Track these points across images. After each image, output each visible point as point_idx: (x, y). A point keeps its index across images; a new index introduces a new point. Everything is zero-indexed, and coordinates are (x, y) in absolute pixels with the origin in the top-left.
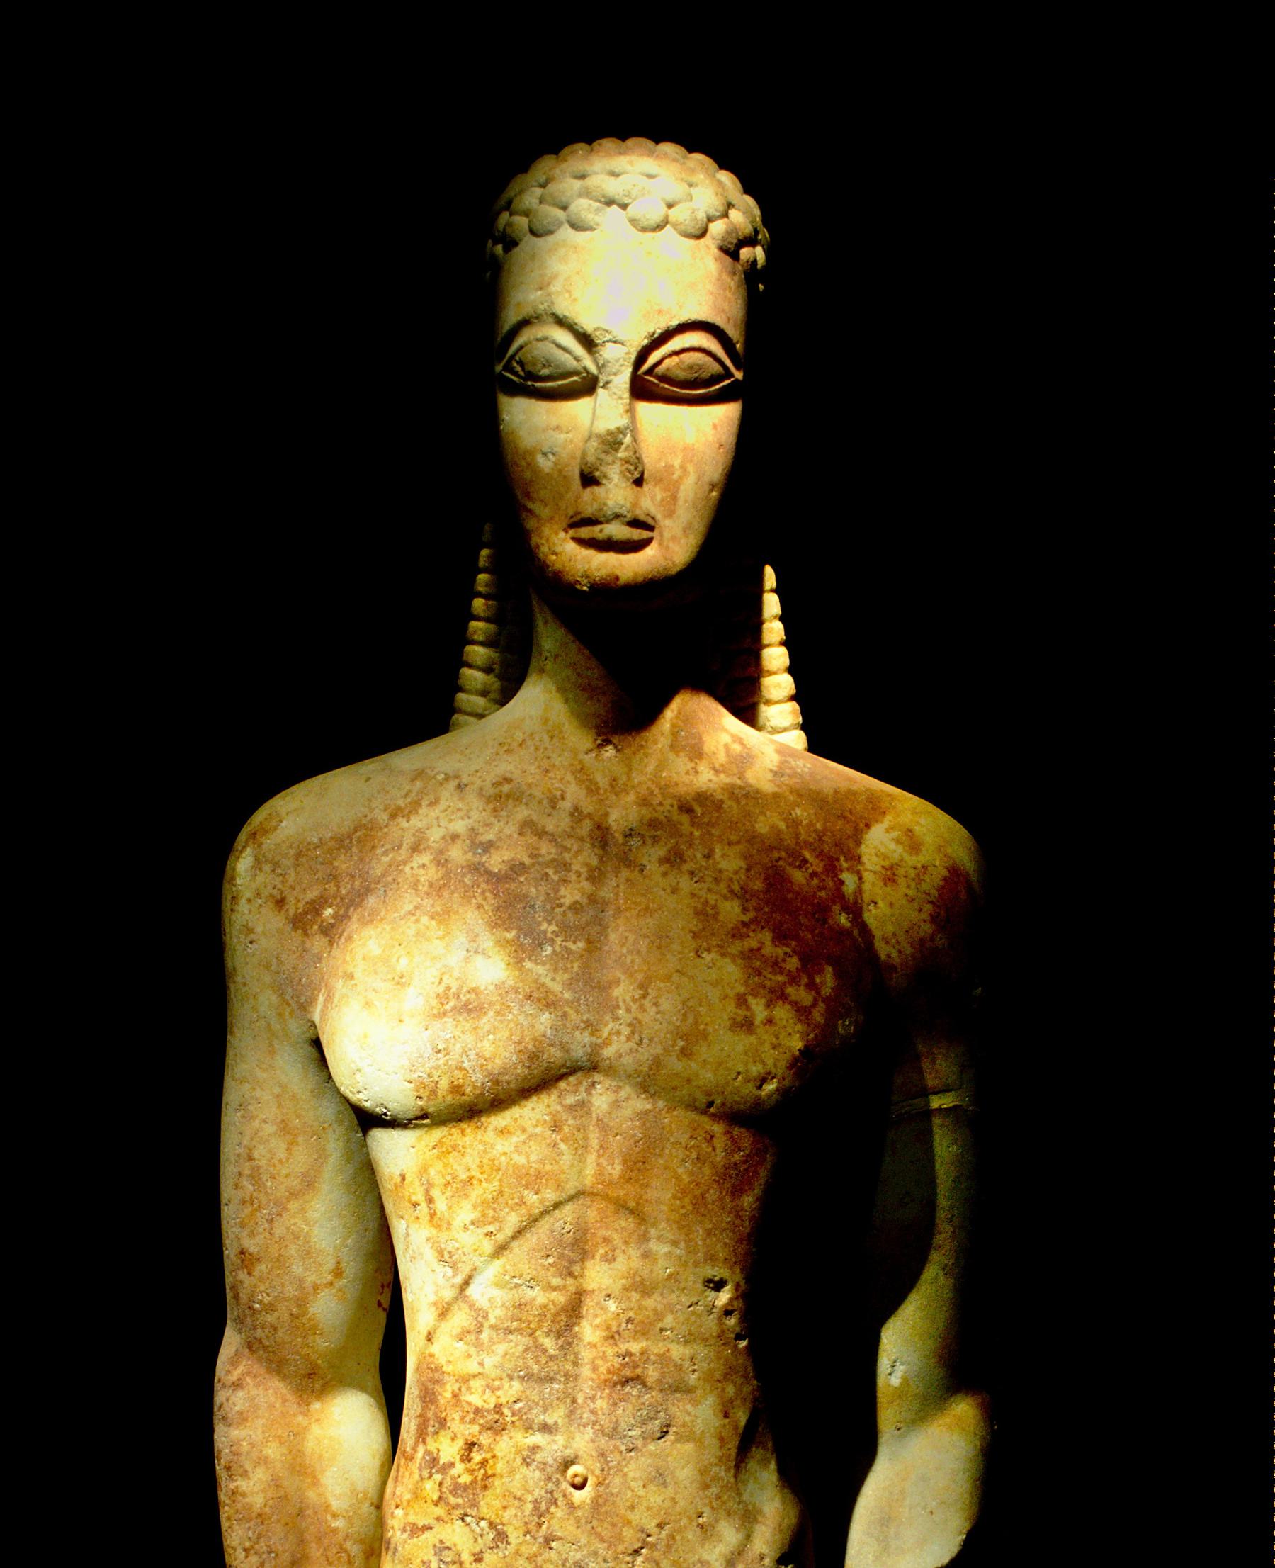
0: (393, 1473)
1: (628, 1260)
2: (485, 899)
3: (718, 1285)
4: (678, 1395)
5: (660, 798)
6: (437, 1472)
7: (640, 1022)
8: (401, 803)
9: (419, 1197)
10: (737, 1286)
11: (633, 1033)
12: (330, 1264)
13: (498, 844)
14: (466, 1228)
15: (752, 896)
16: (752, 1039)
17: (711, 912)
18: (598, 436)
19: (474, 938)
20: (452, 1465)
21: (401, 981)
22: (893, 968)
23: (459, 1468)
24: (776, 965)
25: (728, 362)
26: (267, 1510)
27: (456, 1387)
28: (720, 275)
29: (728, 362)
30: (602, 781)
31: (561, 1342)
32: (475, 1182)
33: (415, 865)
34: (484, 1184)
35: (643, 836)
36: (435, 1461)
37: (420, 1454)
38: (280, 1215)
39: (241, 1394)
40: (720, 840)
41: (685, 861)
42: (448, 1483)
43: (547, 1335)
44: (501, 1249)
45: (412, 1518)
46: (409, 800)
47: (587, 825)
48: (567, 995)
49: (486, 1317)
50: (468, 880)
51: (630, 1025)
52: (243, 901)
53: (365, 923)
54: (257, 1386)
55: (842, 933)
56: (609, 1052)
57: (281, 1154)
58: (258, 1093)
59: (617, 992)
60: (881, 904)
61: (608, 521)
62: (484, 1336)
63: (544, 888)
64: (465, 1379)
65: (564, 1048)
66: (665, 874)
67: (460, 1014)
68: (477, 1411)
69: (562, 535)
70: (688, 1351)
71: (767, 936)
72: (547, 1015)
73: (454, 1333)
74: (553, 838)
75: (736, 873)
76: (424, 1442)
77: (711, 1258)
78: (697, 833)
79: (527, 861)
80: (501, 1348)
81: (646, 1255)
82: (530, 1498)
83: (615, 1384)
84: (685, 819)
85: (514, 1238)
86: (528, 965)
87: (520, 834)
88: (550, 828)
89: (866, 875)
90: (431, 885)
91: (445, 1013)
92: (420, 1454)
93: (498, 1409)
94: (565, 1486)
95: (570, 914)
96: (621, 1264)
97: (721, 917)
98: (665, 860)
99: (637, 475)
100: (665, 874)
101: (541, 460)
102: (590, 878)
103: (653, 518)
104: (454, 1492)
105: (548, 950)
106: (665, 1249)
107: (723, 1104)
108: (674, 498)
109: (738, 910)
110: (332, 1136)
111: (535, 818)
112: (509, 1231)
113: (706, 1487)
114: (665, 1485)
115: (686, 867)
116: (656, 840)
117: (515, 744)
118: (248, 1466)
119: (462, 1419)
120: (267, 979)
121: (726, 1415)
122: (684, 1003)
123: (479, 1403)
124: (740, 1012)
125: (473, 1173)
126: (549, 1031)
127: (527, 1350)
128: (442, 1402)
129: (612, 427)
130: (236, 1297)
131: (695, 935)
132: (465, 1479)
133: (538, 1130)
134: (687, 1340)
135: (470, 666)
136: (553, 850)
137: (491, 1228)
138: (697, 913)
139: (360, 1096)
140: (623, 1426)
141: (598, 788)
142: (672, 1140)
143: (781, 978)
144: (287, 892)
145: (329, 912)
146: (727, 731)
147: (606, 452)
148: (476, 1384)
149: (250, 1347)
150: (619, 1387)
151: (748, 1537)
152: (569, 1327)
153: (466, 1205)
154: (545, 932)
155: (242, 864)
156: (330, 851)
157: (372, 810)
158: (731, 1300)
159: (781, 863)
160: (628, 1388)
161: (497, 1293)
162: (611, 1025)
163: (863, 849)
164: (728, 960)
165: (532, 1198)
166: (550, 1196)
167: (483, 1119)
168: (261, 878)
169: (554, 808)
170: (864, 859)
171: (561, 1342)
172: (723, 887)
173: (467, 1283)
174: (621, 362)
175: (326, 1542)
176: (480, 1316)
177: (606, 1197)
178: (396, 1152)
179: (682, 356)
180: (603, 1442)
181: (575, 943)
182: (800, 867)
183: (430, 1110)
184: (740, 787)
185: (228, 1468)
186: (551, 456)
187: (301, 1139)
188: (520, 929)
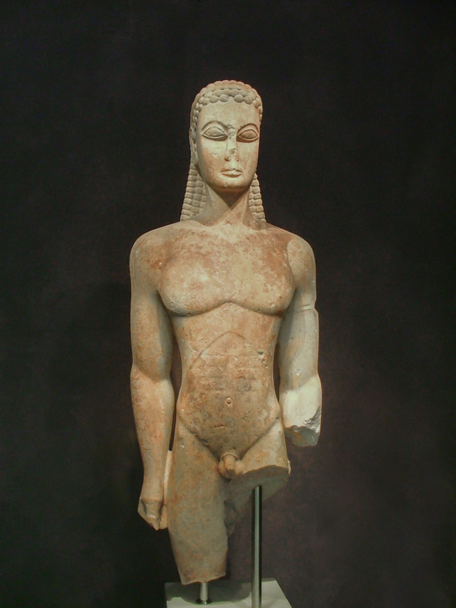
1: (240, 348)
3: (261, 353)
8: (178, 237)
12: (161, 349)
14: (200, 341)
21: (182, 281)
24: (272, 276)
39: (139, 381)
42: (196, 403)
44: (209, 346)
49: (205, 363)
50: (197, 255)
55: (285, 268)
56: (234, 298)
59: (235, 283)
62: (205, 367)
64: (200, 378)
65: (223, 297)
68: (204, 385)
71: (269, 269)
77: (259, 347)
78: (251, 244)
79: (211, 251)
81: (244, 347)
84: (248, 241)
85: (212, 343)
86: (213, 276)
91: (194, 289)
92: (188, 396)
93: (209, 385)
94: (226, 403)
96: (238, 349)
98: (243, 251)
102: (226, 255)
105: (217, 273)
106: (249, 345)
112: (211, 341)
114: (250, 402)
115: (250, 252)
116: (241, 246)
127: (216, 370)
131: (253, 269)
132: (201, 402)
134: (255, 367)
135: (186, 203)
140: (239, 388)
151: (269, 414)
155: (136, 251)
156: (160, 249)
163: (288, 248)
165: (216, 333)
166: (221, 333)
167: (204, 314)
173: (200, 354)
178: (186, 323)
183: (191, 312)
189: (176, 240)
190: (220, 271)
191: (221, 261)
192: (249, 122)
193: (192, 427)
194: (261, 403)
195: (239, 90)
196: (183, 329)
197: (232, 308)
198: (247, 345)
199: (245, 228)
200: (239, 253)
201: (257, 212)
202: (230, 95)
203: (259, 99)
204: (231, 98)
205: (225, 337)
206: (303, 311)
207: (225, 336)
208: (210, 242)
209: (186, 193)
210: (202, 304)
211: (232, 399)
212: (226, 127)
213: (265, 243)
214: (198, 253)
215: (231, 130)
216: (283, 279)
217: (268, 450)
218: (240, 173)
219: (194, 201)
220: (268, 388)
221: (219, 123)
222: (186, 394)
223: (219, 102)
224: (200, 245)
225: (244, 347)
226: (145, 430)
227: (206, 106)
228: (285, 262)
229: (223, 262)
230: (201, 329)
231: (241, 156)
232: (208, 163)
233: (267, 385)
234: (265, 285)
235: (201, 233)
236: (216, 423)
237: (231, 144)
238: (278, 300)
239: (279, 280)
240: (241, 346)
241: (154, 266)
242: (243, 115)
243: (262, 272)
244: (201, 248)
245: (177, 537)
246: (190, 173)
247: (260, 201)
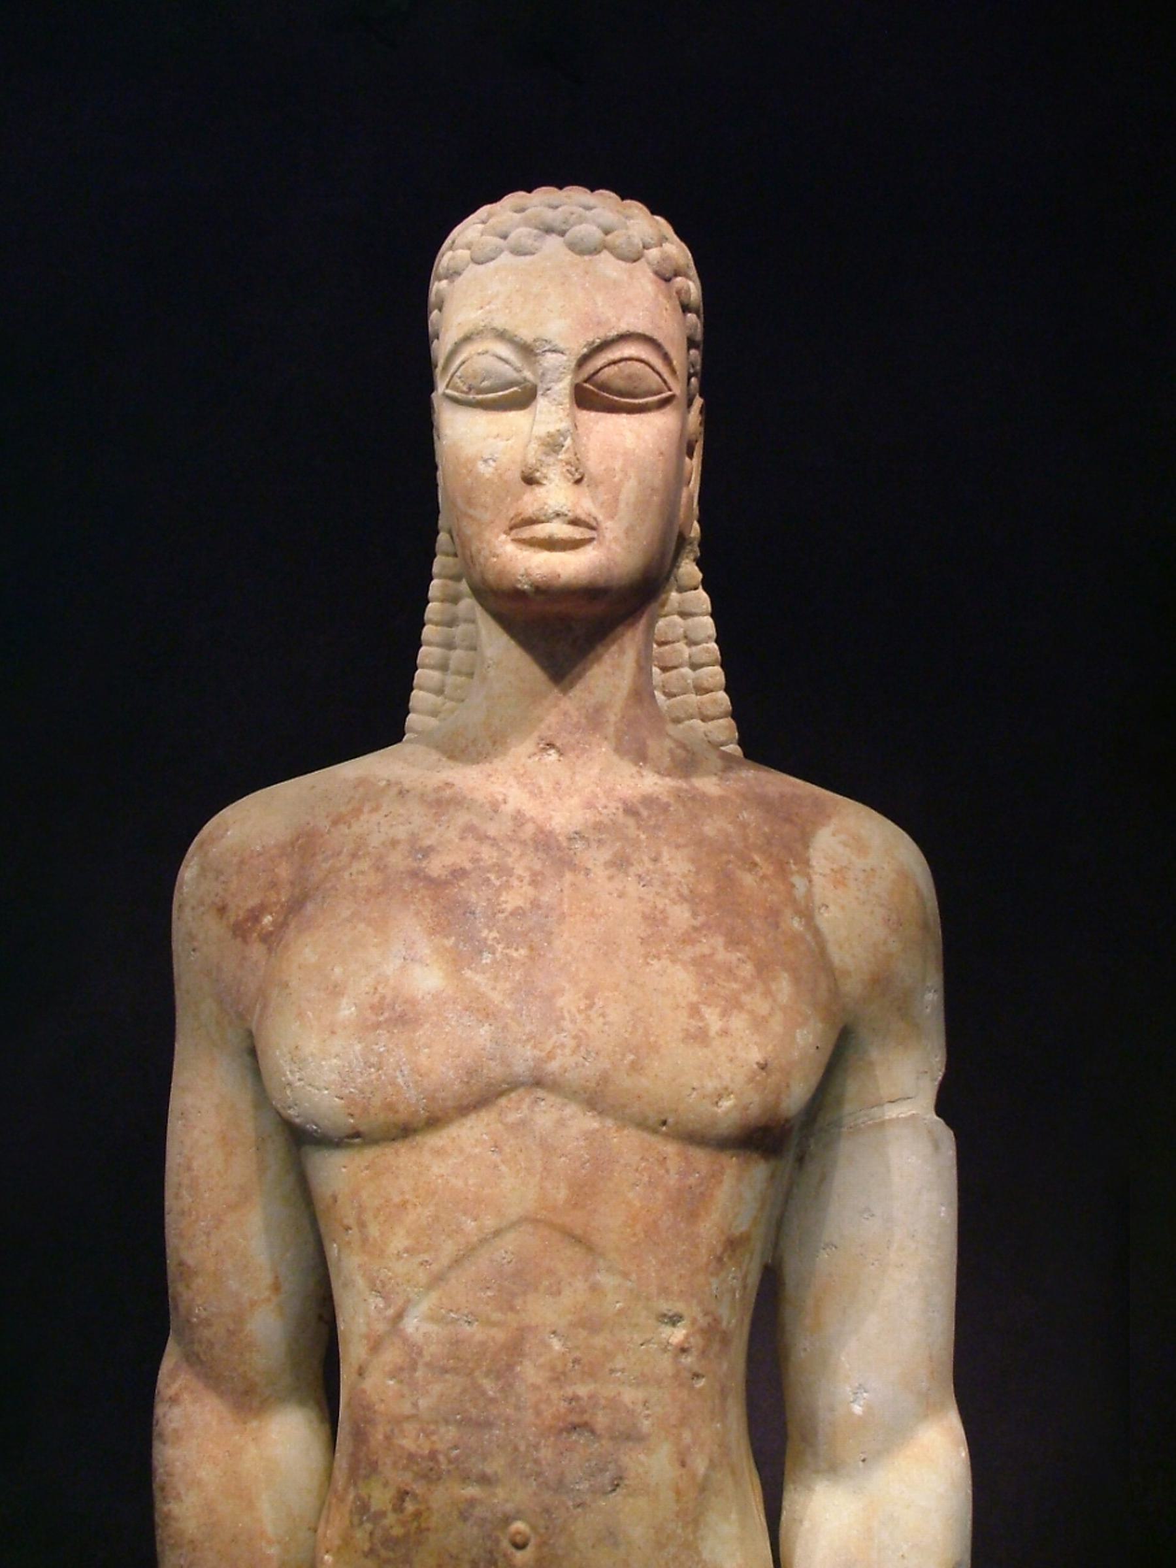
0: (325, 1512)
1: (575, 1293)
2: (424, 904)
3: (674, 1320)
4: (631, 1444)
5: (604, 801)
6: (368, 1520)
7: (586, 1034)
8: (343, 809)
10: (694, 1321)
11: (578, 1046)
12: (267, 1279)
13: (440, 849)
15: (702, 900)
17: (659, 916)
18: (539, 438)
20: (382, 1514)
21: (336, 991)
22: (847, 973)
23: (391, 1519)
24: (730, 972)
25: (666, 375)
27: (388, 1428)
28: (656, 296)
29: (666, 375)
30: (545, 784)
31: (500, 1384)
32: (409, 1206)
33: (354, 870)
34: (419, 1209)
35: (587, 840)
38: (217, 1228)
41: (632, 865)
42: (379, 1533)
43: (487, 1374)
44: (437, 1280)
46: (350, 807)
48: (509, 1006)
49: (420, 1354)
51: (575, 1037)
52: (187, 910)
55: (794, 940)
56: (553, 1066)
59: (561, 1002)
60: (832, 908)
61: (548, 521)
64: (398, 1421)
65: (505, 1062)
66: (611, 878)
67: (395, 1026)
68: (411, 1457)
69: (503, 537)
70: (640, 1395)
71: (719, 941)
72: (486, 1027)
73: (387, 1369)
74: (494, 842)
75: (684, 876)
76: (355, 1484)
77: (664, 1291)
78: (643, 837)
79: (468, 866)
80: (437, 1388)
81: (594, 1288)
83: (561, 1431)
84: (631, 822)
86: (468, 973)
87: (462, 839)
88: (492, 832)
89: (815, 878)
90: (369, 891)
91: (378, 1026)
92: (351, 1497)
93: (433, 1456)
94: (505, 1544)
96: (568, 1298)
97: (670, 922)
99: (577, 476)
100: (611, 878)
101: (481, 467)
102: (534, 883)
103: (595, 519)
105: (487, 958)
107: (677, 1123)
108: (616, 500)
109: (687, 915)
112: (445, 1261)
113: (661, 1546)
114: (616, 1544)
115: (633, 870)
116: (600, 842)
118: (181, 1488)
119: (395, 1463)
122: (632, 1013)
124: (693, 1022)
125: (407, 1197)
126: (488, 1045)
127: (464, 1391)
129: (552, 429)
130: (176, 1307)
131: (643, 941)
132: (397, 1531)
134: (642, 1381)
135: (421, 688)
136: (495, 854)
137: (426, 1257)
138: (645, 917)
139: (291, 1112)
141: (541, 792)
142: (622, 1161)
145: (267, 919)
146: (670, 736)
147: (547, 454)
148: (410, 1428)
149: (187, 1360)
150: (565, 1434)
152: (510, 1367)
154: (486, 939)
155: (189, 872)
158: (687, 1337)
159: (730, 866)
160: (574, 1437)
161: (432, 1328)
162: (555, 1037)
164: (678, 967)
165: (470, 1225)
167: (418, 1138)
169: (496, 811)
170: (814, 863)
171: (500, 1384)
173: (400, 1316)
174: (561, 369)
176: (414, 1352)
177: (551, 1225)
179: (622, 364)
180: (547, 1496)
181: (517, 950)
182: (750, 870)
183: (363, 1128)
184: (686, 791)
185: (162, 1489)
186: (491, 462)
190: (500, 947)
191: (509, 907)
192: (623, 327)
194: (672, 1550)
195: (588, 208)
196: (335, 1199)
197: (546, 1114)
198: (607, 1280)
199: (626, 768)
200: (588, 871)
201: (705, 719)
202: (549, 230)
203: (677, 250)
204: (554, 241)
205: (510, 1242)
206: (882, 1124)
207: (510, 1236)
208: (470, 829)
209: (423, 649)
210: (412, 1094)
211: (534, 1528)
212: (528, 351)
214: (414, 874)
215: (550, 360)
216: (784, 987)
218: (593, 534)
219: (451, 679)
220: (706, 1477)
221: (502, 335)
222: (346, 1490)
223: (506, 258)
224: (427, 843)
225: (594, 1288)
227: (459, 280)
229: (517, 913)
230: (404, 1204)
231: (594, 464)
232: (460, 502)
233: (700, 1465)
235: (438, 789)
237: (551, 413)
238: (751, 1080)
239: (760, 988)
240: (580, 1284)
241: (242, 930)
242: (599, 299)
243: (689, 952)
244: (427, 852)
246: (436, 569)
247: (715, 674)
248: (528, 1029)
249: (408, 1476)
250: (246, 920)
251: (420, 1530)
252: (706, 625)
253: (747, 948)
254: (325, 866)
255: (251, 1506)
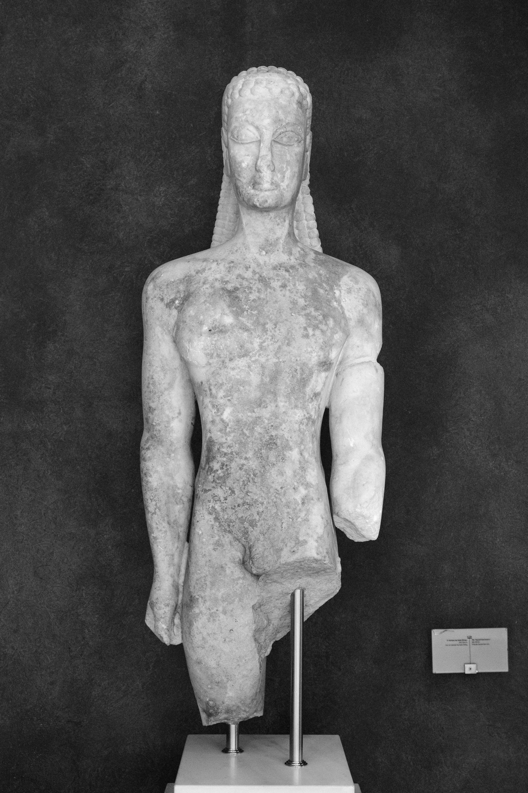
8: (199, 269)
9: (207, 389)
14: (222, 398)
16: (309, 340)
19: (223, 310)
21: (201, 324)
26: (158, 487)
36: (212, 469)
37: (207, 467)
39: (149, 451)
40: (298, 281)
42: (216, 476)
43: (247, 430)
45: (204, 487)
47: (257, 275)
48: (252, 327)
49: (228, 425)
50: (221, 292)
52: (150, 299)
53: (188, 306)
54: (154, 449)
55: (335, 309)
57: (162, 377)
58: (155, 358)
59: (267, 326)
63: (244, 294)
64: (221, 444)
71: (312, 309)
75: (303, 290)
76: (209, 464)
78: (291, 278)
79: (239, 287)
80: (232, 435)
82: (242, 480)
84: (287, 274)
86: (240, 318)
88: (246, 277)
89: (342, 291)
90: (210, 294)
92: (207, 467)
95: (252, 303)
100: (281, 291)
102: (258, 292)
104: (218, 479)
109: (304, 301)
110: (178, 371)
111: (241, 273)
114: (283, 475)
115: (288, 288)
117: (234, 251)
118: (152, 473)
119: (220, 457)
120: (158, 323)
121: (301, 454)
123: (226, 451)
128: (214, 451)
130: (148, 422)
132: (222, 475)
133: (243, 368)
135: (218, 226)
137: (229, 398)
143: (317, 322)
144: (164, 296)
145: (177, 302)
153: (222, 391)
156: (177, 283)
157: (190, 271)
168: (156, 292)
172: (299, 295)
175: (176, 497)
185: (145, 474)
187: (168, 372)
188: (237, 307)
189: (197, 273)
190: (249, 311)
193: (211, 506)
194: (298, 477)
208: (239, 276)
213: (310, 277)
217: (305, 538)
222: (205, 466)
224: (226, 280)
226: (155, 513)
228: (336, 301)
229: (254, 301)
234: (305, 329)
236: (240, 501)
239: (324, 322)
240: (273, 405)
242: (280, 112)
243: (303, 313)
245: (193, 655)
248: (258, 334)
249: (225, 459)
250: (170, 302)
251: (228, 474)
252: (311, 209)
253: (321, 311)
254: (195, 286)
255: (173, 478)
